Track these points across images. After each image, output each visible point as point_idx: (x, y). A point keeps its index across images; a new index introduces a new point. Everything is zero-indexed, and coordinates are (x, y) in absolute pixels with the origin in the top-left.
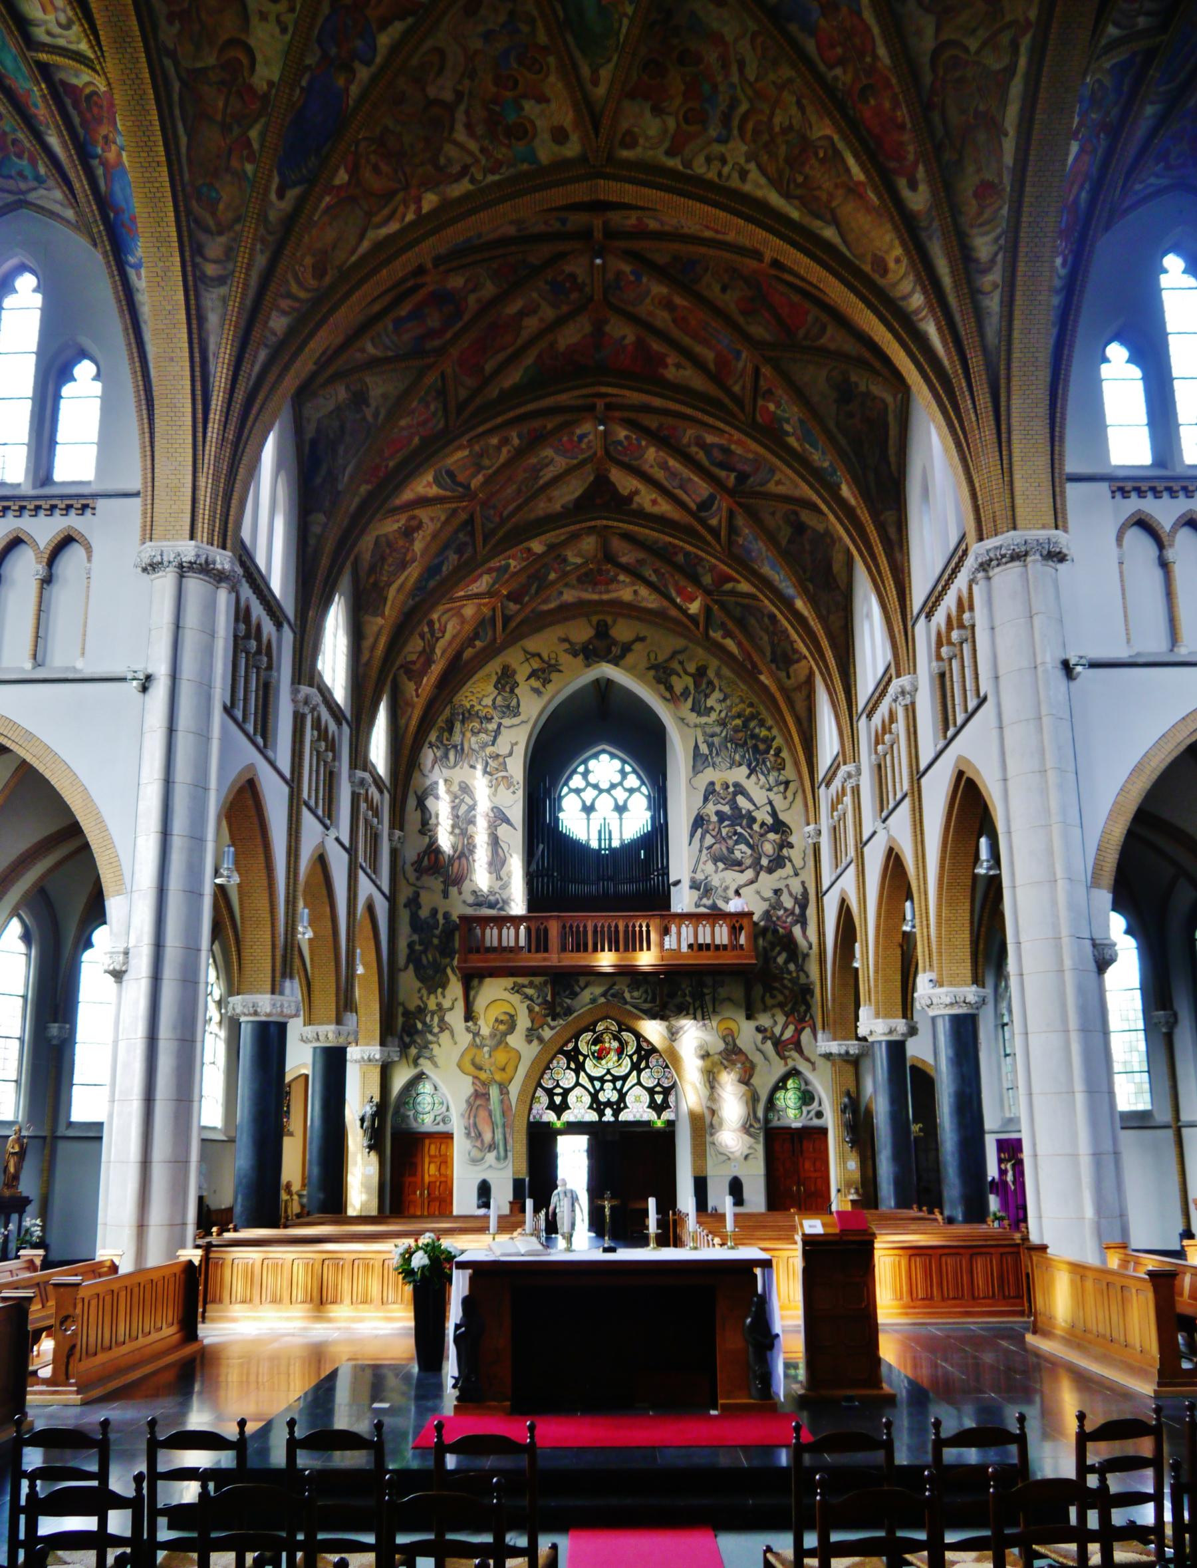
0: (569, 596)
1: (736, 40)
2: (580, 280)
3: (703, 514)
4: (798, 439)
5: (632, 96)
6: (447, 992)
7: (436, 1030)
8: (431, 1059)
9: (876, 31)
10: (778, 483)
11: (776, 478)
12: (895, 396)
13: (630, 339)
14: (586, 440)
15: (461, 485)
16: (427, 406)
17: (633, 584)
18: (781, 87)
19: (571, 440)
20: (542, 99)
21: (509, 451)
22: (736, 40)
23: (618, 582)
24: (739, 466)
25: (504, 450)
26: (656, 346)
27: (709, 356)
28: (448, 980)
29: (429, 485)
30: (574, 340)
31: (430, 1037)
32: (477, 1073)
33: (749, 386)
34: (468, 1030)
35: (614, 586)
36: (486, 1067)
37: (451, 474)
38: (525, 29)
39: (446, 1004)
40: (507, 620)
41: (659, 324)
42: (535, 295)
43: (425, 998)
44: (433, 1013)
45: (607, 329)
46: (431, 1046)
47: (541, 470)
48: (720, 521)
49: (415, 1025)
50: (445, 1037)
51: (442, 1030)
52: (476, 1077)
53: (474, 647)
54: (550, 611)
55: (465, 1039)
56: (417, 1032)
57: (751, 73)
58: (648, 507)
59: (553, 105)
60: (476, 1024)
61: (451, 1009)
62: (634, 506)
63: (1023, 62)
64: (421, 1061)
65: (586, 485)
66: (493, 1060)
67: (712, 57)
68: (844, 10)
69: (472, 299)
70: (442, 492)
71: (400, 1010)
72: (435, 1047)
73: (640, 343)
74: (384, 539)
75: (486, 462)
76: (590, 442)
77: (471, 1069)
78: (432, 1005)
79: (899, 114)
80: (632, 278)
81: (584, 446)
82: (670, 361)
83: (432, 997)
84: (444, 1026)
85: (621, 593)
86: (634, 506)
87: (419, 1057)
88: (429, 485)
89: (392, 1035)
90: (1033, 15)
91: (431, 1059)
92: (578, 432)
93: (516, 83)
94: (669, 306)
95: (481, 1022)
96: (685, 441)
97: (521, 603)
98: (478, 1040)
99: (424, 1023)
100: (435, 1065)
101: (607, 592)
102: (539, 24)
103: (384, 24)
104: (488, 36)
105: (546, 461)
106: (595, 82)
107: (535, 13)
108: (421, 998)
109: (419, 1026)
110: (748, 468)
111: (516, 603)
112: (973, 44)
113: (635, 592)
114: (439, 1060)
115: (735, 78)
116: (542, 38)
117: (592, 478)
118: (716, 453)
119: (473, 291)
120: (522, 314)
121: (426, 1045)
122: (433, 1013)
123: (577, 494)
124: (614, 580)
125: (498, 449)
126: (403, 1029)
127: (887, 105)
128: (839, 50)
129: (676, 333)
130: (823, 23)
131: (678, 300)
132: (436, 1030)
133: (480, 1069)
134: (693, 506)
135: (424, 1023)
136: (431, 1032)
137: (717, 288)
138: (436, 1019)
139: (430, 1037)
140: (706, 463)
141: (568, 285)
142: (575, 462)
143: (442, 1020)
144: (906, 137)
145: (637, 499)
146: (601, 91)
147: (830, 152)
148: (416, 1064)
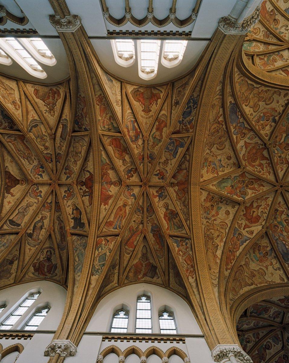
1: (219, 218)
2: (130, 178)
3: (8, 222)
4: (98, 254)
5: (209, 194)
9: (240, 250)
10: (30, 250)
11: (32, 248)
12: (116, 283)
13: (111, 194)
14: (39, 177)
15: (31, 129)
16: (108, 125)
18: (217, 230)
19: (40, 171)
20: (207, 172)
21: (42, 149)
22: (219, 218)
24: (35, 234)
25: (43, 147)
26: (110, 201)
27: (112, 219)
29: (33, 117)
30: (111, 176)
33: (106, 234)
37: (36, 126)
38: (221, 169)
41: (118, 202)
42: (129, 165)
45: (112, 186)
47: (27, 159)
48: (5, 230)
57: (215, 222)
58: (6, 201)
59: (206, 174)
62: (6, 195)
63: (252, 287)
65: (15, 176)
67: (214, 212)
68: (239, 242)
69: (135, 146)
70: (29, 121)
73: (110, 197)
74: (13, 92)
75: (39, 140)
76: (39, 178)
79: (232, 261)
80: (132, 194)
81: (36, 176)
82: (107, 206)
86: (6, 195)
88: (33, 117)
90: (259, 285)
92: (43, 175)
93: (209, 166)
94: (125, 205)
96: (43, 212)
102: (223, 173)
103: (237, 138)
104: (220, 161)
105: (31, 162)
106: (212, 185)
107: (225, 172)
110: (34, 237)
112: (246, 274)
115: (213, 219)
116: (220, 173)
117: (18, 178)
118: (40, 224)
119: (137, 147)
120: (124, 160)
123: (12, 173)
125: (44, 145)
127: (232, 257)
128: (233, 243)
129: (117, 207)
130: (235, 238)
131: (128, 208)
134: (11, 218)
137: (134, 219)
140: (35, 221)
141: (129, 175)
142: (30, 173)
144: (230, 264)
145: (10, 195)
146: (211, 187)
147: (216, 246)
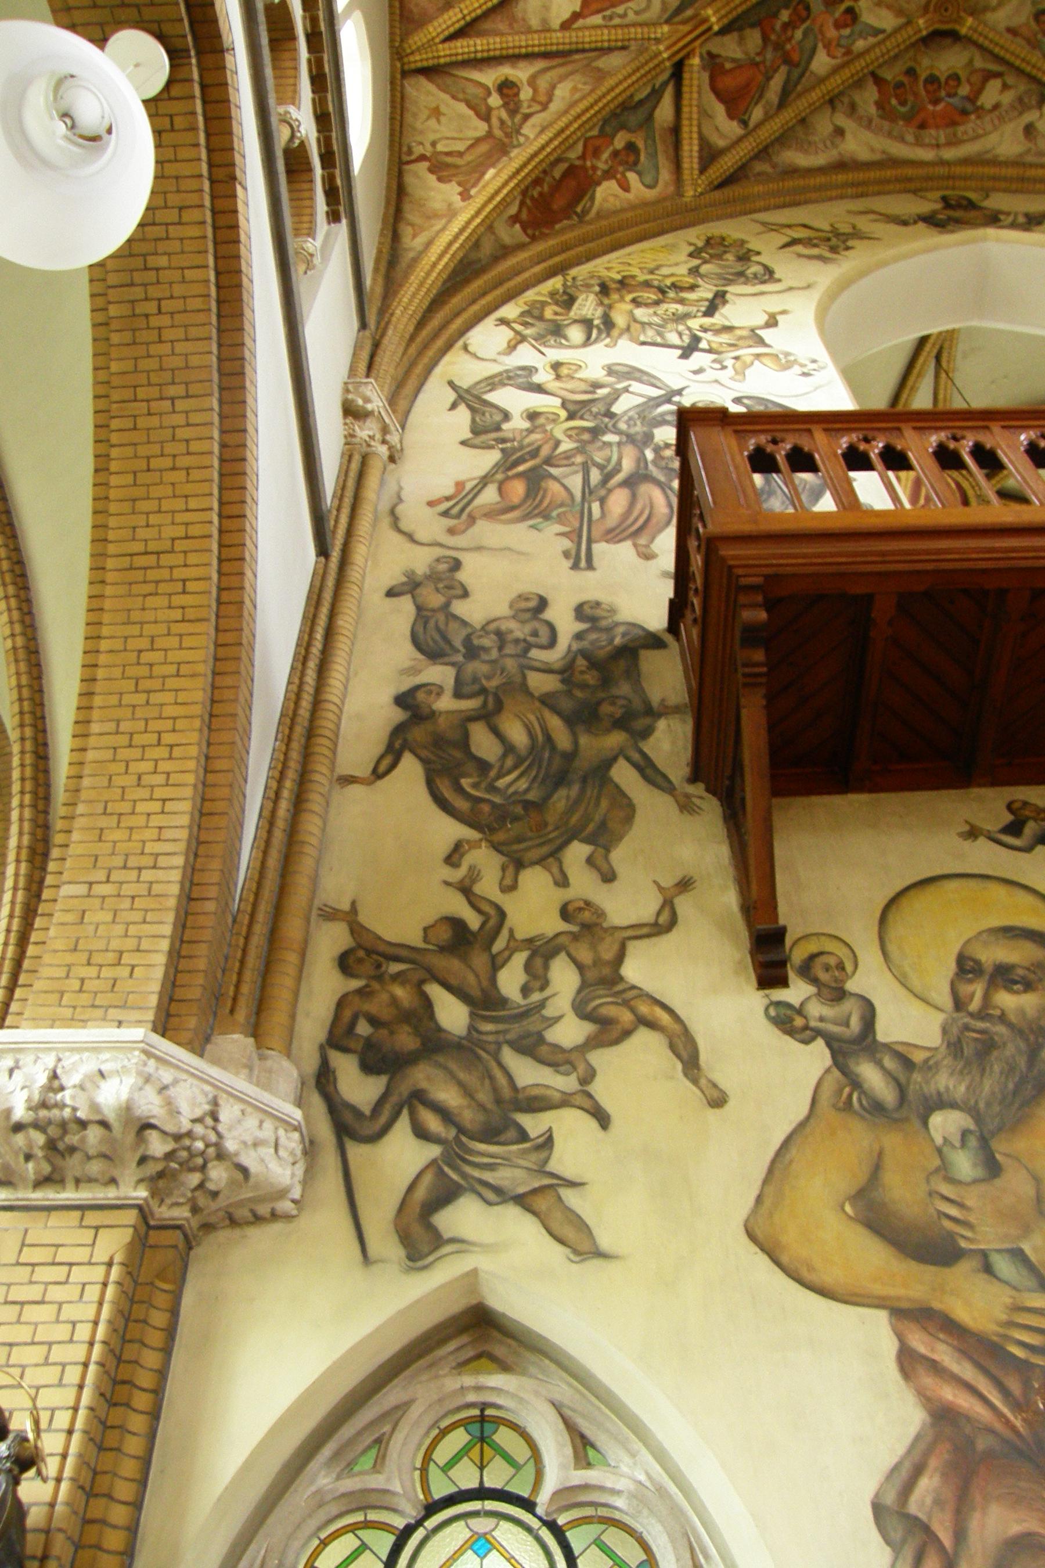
0: (860, 143)
6: (618, 856)
7: (569, 1032)
8: (545, 1199)
17: (1021, 105)
23: (979, 111)
28: (627, 810)
31: (527, 1073)
32: (915, 1282)
34: (787, 1022)
35: (971, 125)
36: (988, 1235)
39: (627, 903)
40: (709, 155)
43: (488, 887)
44: (541, 953)
46: (534, 1124)
49: (428, 1004)
50: (633, 1072)
51: (608, 1033)
52: (907, 1315)
53: (626, 188)
54: (810, 171)
55: (776, 1076)
56: (435, 1044)
60: (839, 994)
61: (663, 924)
64: (464, 1217)
66: (1016, 1184)
71: (331, 940)
72: (569, 1127)
77: (869, 1258)
78: (533, 906)
83: (536, 882)
84: (616, 1011)
85: (993, 139)
87: (445, 1195)
89: (256, 1031)
91: (545, 1199)
95: (870, 979)
97: (744, 123)
98: (870, 1075)
99: (485, 1002)
100: (580, 1243)
101: (953, 142)
108: (466, 890)
109: (452, 1014)
111: (731, 116)
113: (1029, 130)
114: (612, 1209)
121: (504, 1117)
122: (541, 953)
124: (970, 108)
126: (338, 1038)
132: (569, 1032)
133: (934, 1249)
135: (485, 1002)
136: (532, 1046)
138: (564, 979)
139: (527, 1073)
143: (604, 979)
148: (420, 1234)
